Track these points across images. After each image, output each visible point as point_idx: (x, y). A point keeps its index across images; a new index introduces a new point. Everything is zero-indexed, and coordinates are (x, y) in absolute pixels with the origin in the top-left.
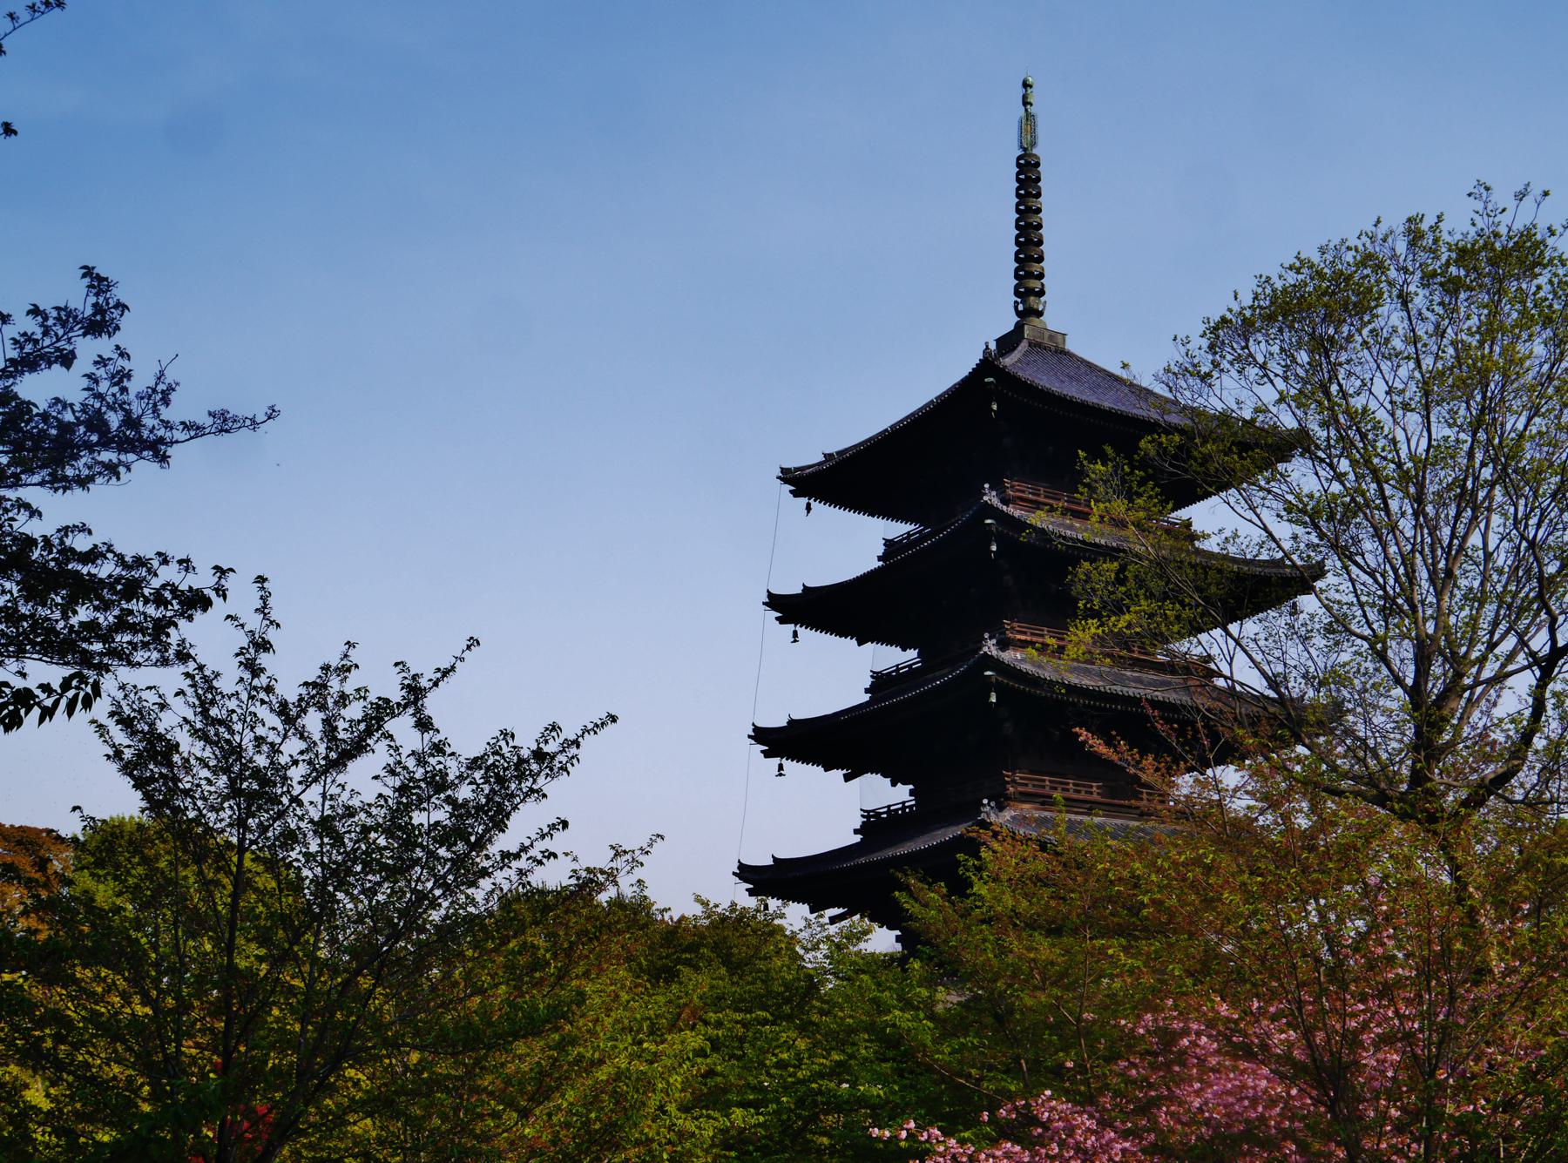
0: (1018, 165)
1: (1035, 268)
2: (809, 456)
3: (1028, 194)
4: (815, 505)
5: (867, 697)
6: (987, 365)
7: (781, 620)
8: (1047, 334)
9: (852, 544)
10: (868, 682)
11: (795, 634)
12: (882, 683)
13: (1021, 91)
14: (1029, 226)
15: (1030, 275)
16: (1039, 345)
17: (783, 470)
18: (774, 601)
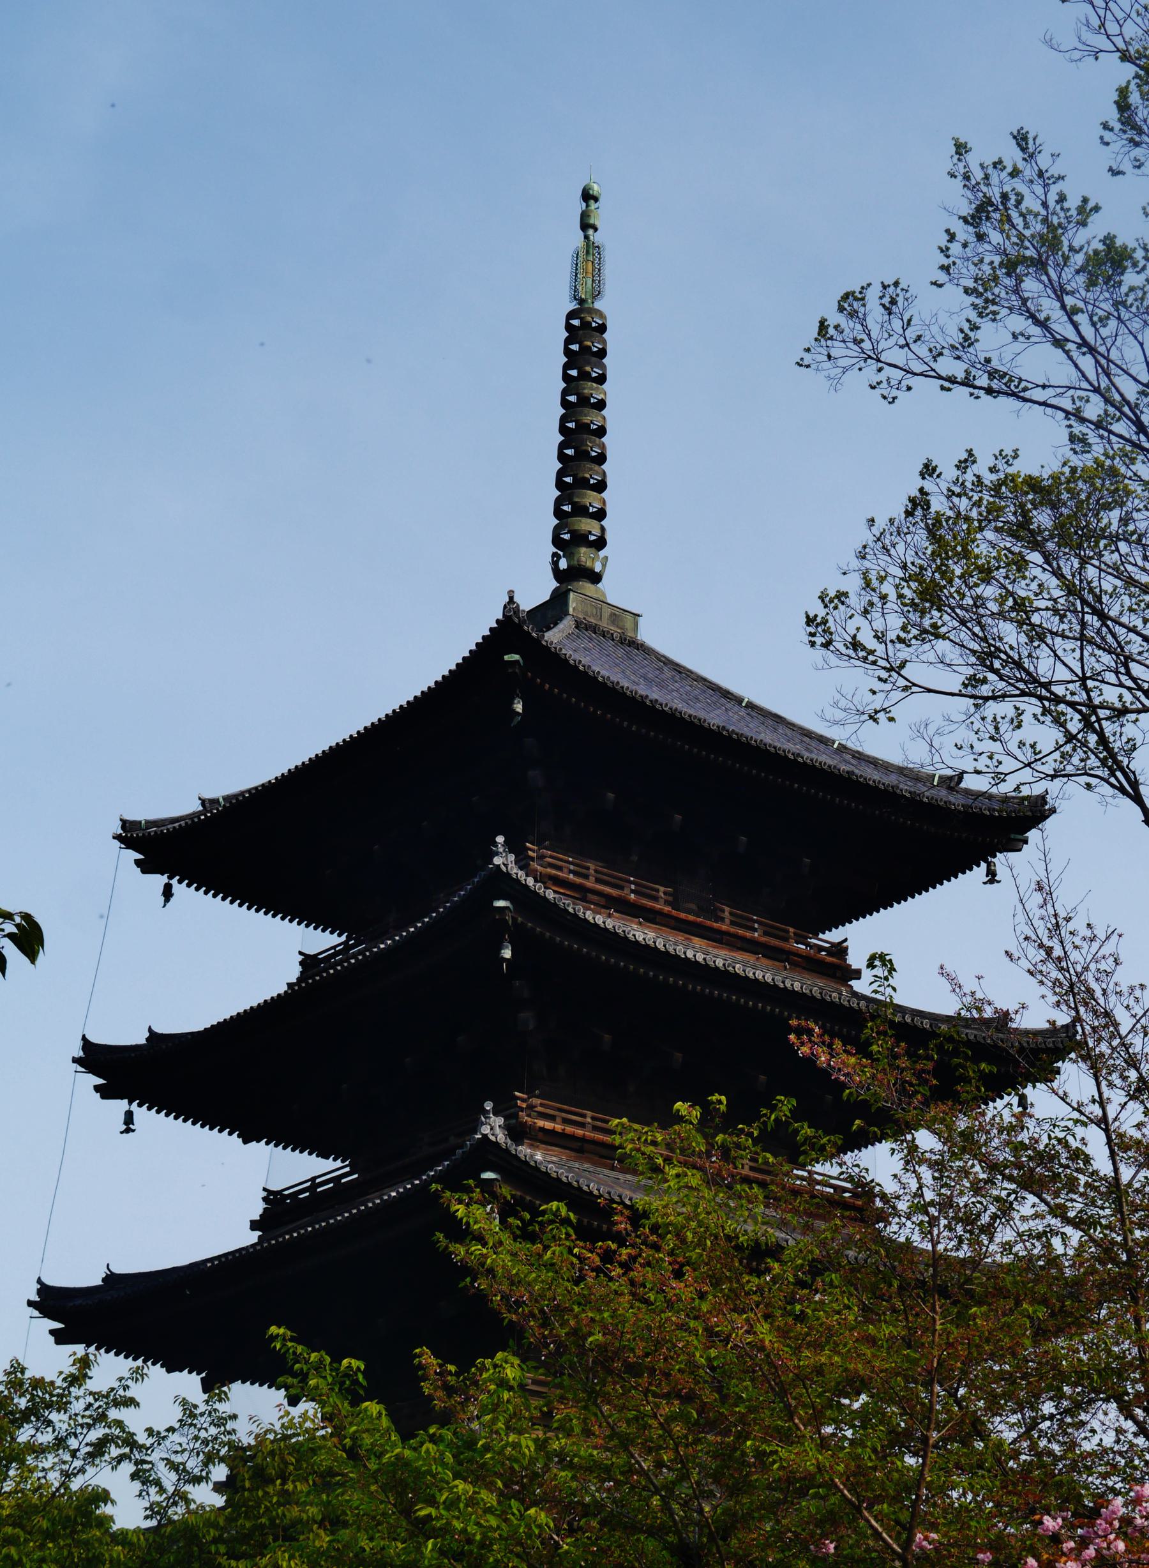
0: (569, 327)
1: (592, 500)
2: (176, 801)
3: (584, 376)
4: (180, 889)
5: (253, 1237)
6: (512, 630)
7: (105, 1092)
8: (607, 612)
9: (239, 959)
10: (257, 1209)
11: (129, 1118)
12: (279, 1208)
13: (579, 206)
14: (583, 428)
15: (581, 511)
16: (594, 629)
17: (125, 824)
18: (94, 1057)
